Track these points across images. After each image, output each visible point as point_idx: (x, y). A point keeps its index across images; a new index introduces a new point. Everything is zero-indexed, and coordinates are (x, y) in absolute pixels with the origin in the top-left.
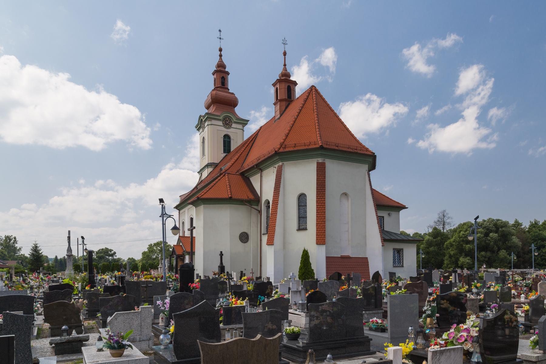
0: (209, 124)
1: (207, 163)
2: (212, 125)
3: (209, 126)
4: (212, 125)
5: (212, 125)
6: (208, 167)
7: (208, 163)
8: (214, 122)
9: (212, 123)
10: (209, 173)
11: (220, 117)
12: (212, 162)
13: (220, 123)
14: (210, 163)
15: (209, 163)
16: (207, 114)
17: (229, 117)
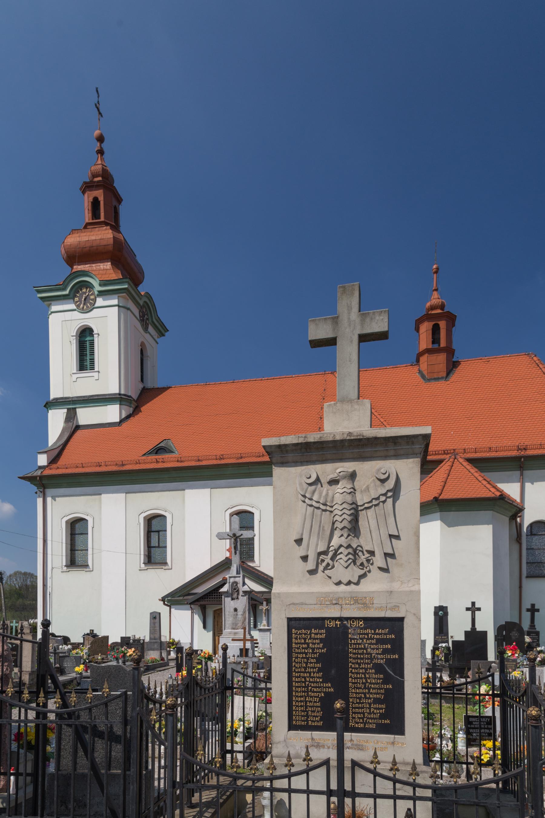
0: (121, 305)
1: (117, 392)
2: (129, 311)
3: (122, 309)
4: (128, 309)
5: (128, 309)
6: (120, 401)
7: (120, 394)
8: (131, 304)
9: (128, 307)
10: (124, 416)
11: (141, 299)
12: (129, 394)
13: (136, 311)
14: (124, 395)
15: (122, 392)
16: (129, 284)
17: (147, 307)
